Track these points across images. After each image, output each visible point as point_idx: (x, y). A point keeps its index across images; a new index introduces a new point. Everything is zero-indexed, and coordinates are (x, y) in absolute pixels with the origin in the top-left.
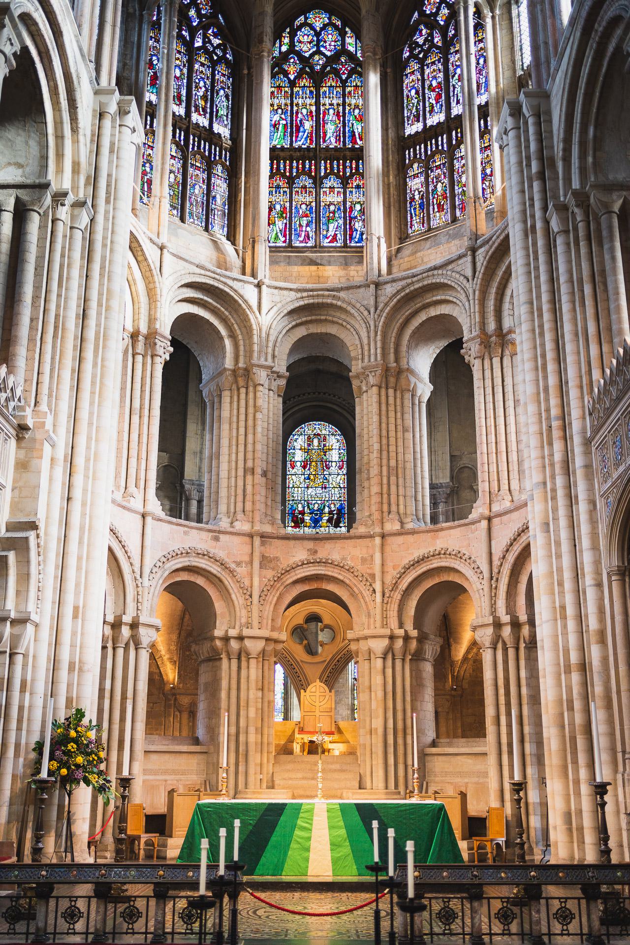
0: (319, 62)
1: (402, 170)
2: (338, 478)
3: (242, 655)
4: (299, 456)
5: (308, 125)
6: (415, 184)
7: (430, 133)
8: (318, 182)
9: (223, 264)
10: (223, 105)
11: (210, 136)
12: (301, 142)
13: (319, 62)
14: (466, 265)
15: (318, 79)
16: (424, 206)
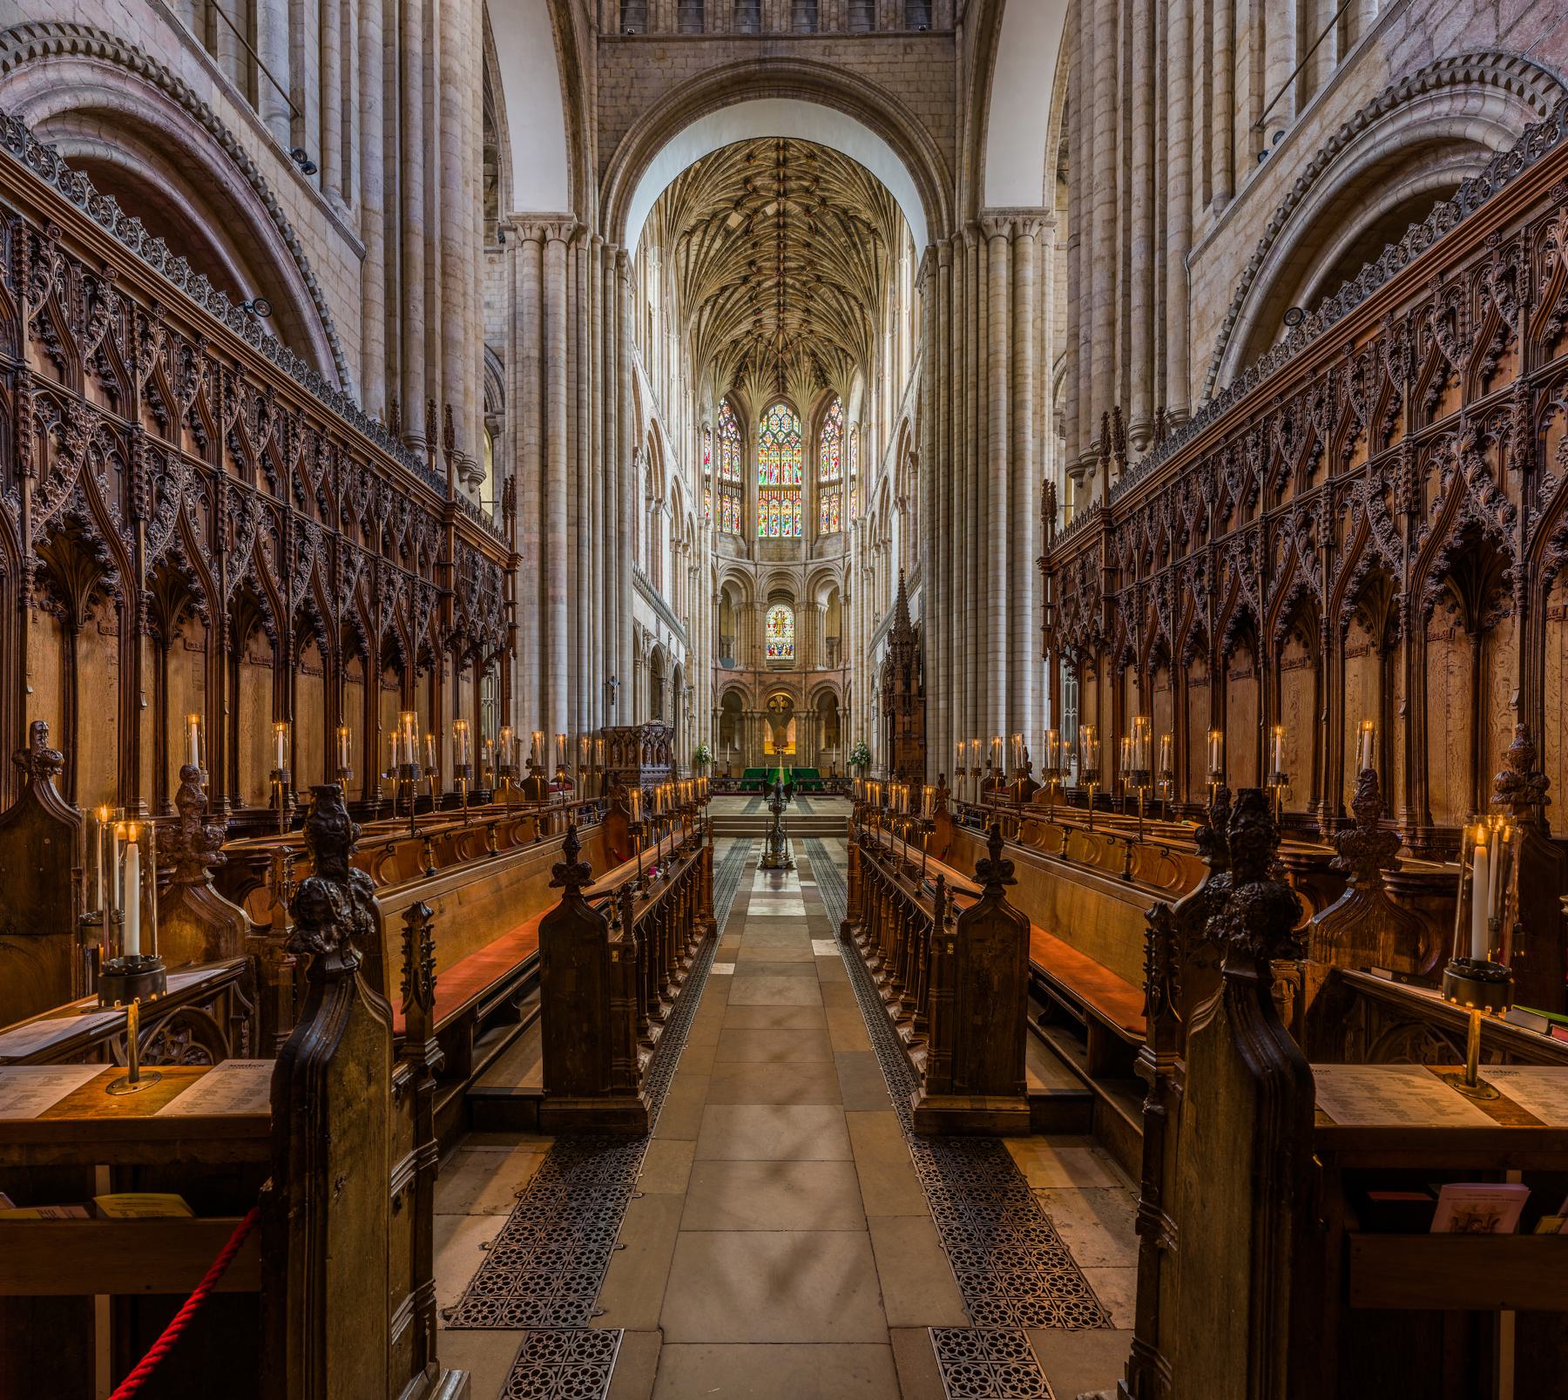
0: (781, 437)
1: (819, 499)
2: (789, 632)
3: (753, 718)
4: (772, 622)
5: (776, 472)
6: (824, 508)
7: (831, 484)
8: (780, 502)
9: (739, 553)
10: (736, 463)
11: (731, 484)
12: (773, 483)
13: (781, 437)
14: (840, 562)
15: (780, 446)
16: (828, 519)
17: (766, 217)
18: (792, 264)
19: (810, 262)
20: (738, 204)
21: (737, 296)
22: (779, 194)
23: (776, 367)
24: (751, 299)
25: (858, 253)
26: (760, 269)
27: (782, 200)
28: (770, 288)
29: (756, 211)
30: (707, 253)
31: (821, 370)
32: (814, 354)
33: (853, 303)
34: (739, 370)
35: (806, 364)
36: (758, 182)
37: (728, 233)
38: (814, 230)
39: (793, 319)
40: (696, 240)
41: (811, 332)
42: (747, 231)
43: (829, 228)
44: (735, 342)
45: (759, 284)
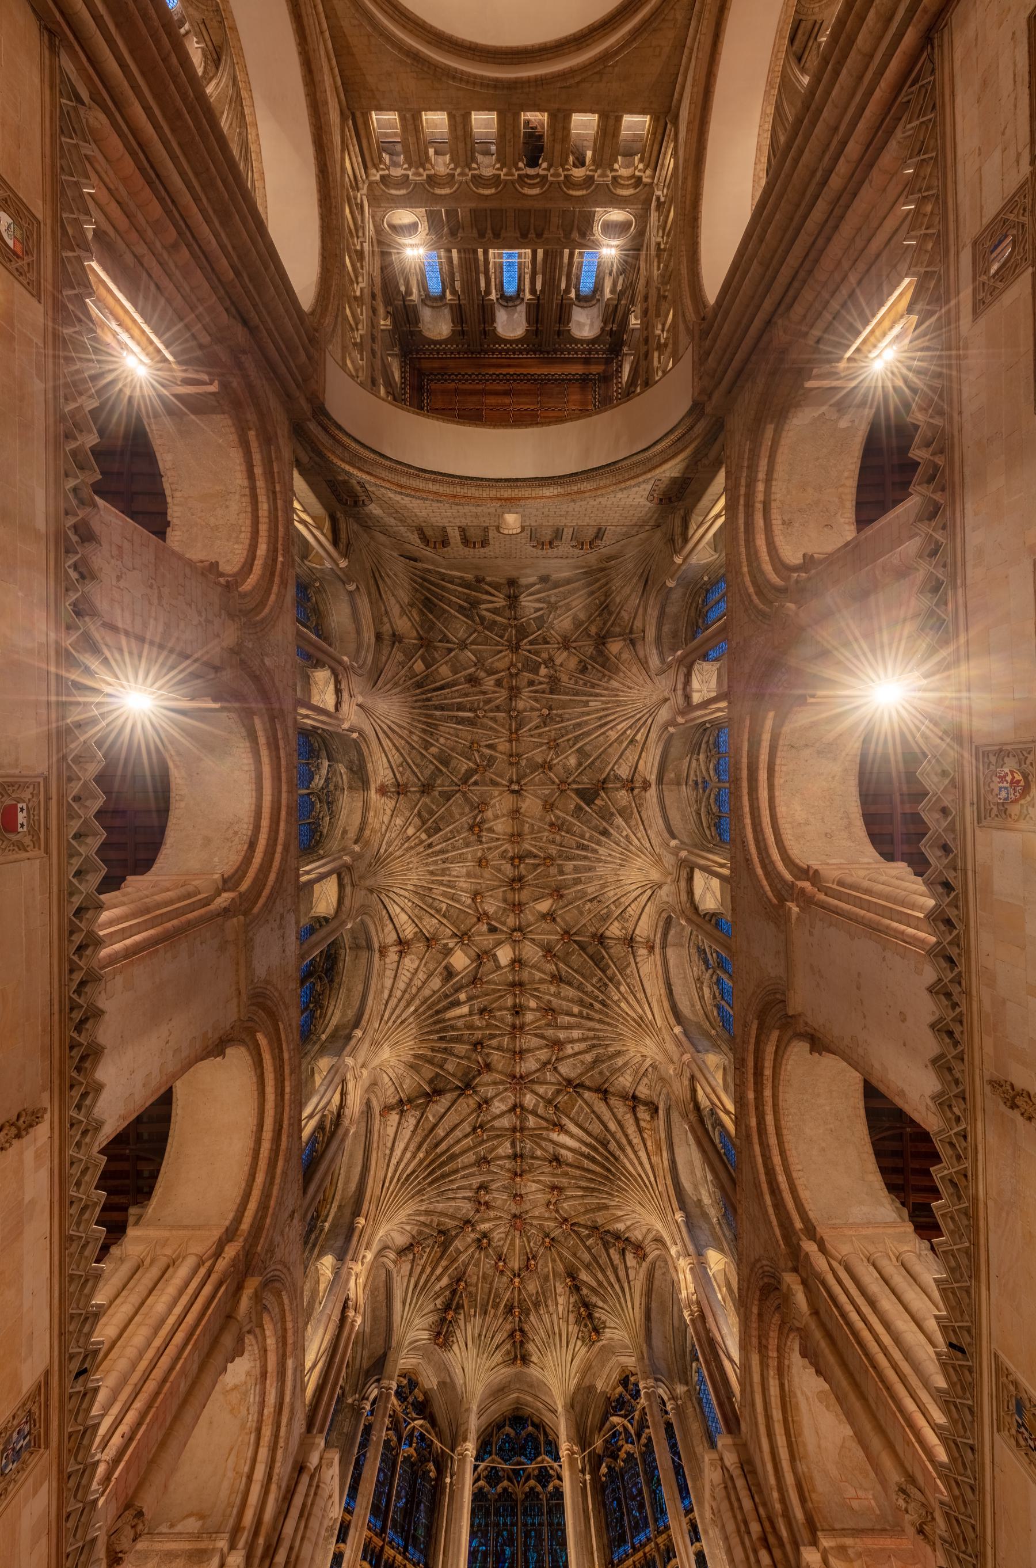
17: (499, 967)
18: (530, 1064)
19: (557, 1044)
20: (463, 937)
21: (452, 1118)
22: (514, 930)
23: (509, 1309)
24: (474, 1129)
25: (617, 986)
26: (488, 1067)
27: (517, 935)
28: (502, 1114)
29: (486, 952)
30: (419, 989)
31: (586, 1305)
32: (572, 1274)
33: (621, 1109)
34: (447, 1307)
35: (563, 1300)
36: (491, 906)
37: (449, 973)
38: (558, 979)
39: (533, 1189)
40: (410, 963)
41: (566, 1220)
42: (475, 980)
43: (575, 971)
44: (444, 1237)
45: (487, 1101)
